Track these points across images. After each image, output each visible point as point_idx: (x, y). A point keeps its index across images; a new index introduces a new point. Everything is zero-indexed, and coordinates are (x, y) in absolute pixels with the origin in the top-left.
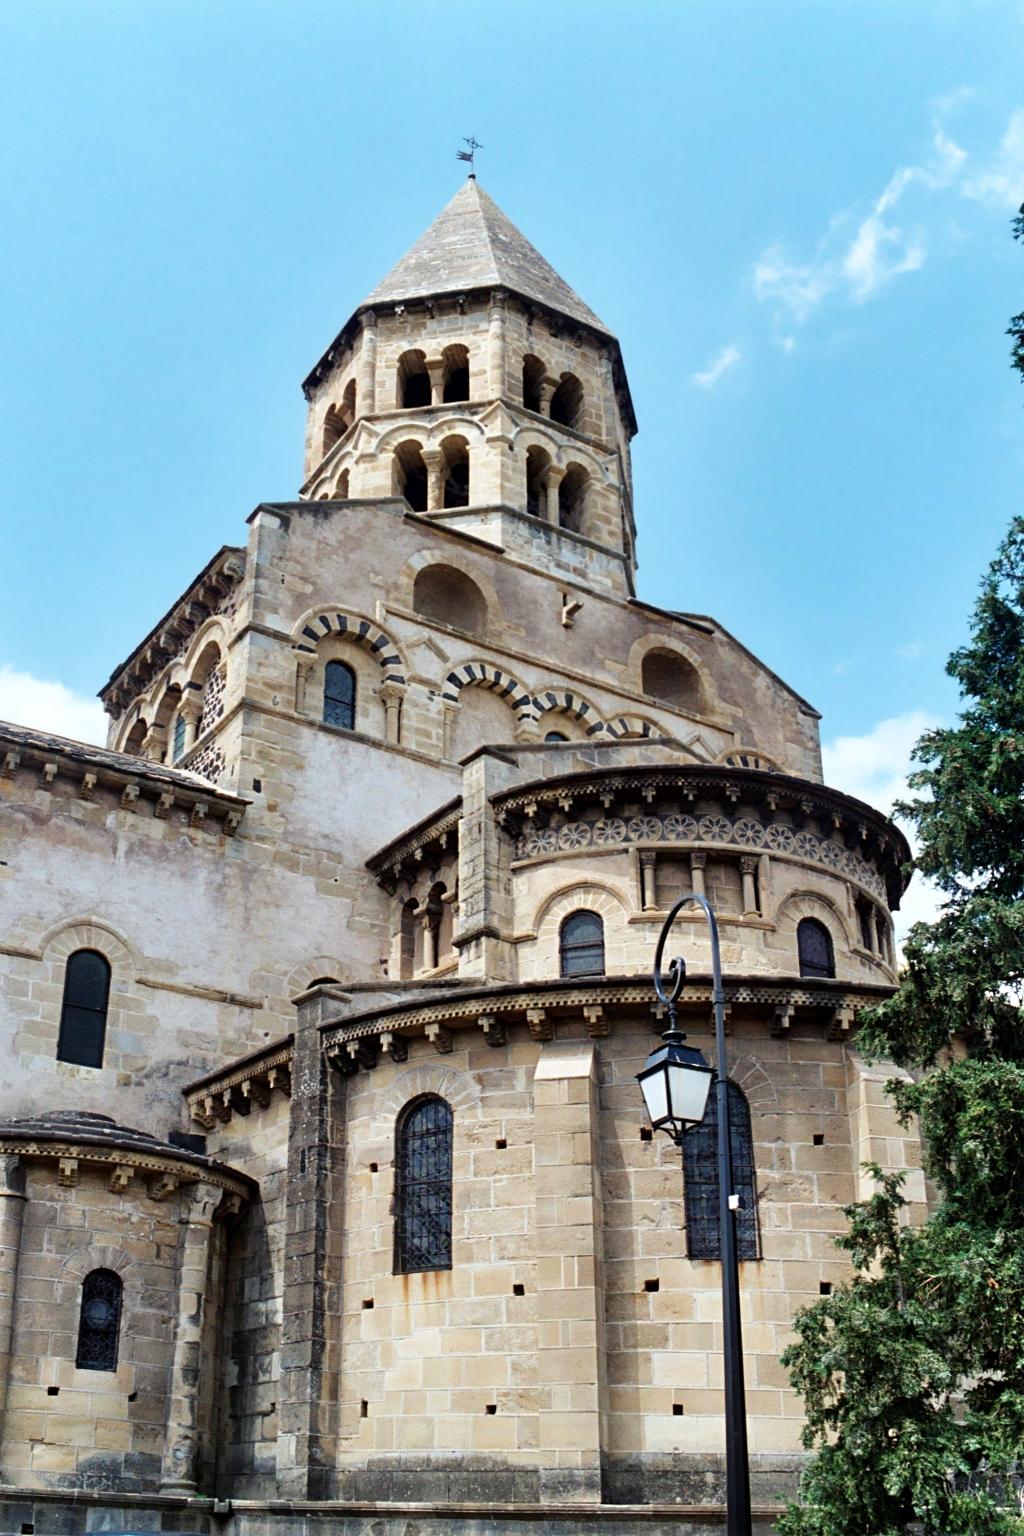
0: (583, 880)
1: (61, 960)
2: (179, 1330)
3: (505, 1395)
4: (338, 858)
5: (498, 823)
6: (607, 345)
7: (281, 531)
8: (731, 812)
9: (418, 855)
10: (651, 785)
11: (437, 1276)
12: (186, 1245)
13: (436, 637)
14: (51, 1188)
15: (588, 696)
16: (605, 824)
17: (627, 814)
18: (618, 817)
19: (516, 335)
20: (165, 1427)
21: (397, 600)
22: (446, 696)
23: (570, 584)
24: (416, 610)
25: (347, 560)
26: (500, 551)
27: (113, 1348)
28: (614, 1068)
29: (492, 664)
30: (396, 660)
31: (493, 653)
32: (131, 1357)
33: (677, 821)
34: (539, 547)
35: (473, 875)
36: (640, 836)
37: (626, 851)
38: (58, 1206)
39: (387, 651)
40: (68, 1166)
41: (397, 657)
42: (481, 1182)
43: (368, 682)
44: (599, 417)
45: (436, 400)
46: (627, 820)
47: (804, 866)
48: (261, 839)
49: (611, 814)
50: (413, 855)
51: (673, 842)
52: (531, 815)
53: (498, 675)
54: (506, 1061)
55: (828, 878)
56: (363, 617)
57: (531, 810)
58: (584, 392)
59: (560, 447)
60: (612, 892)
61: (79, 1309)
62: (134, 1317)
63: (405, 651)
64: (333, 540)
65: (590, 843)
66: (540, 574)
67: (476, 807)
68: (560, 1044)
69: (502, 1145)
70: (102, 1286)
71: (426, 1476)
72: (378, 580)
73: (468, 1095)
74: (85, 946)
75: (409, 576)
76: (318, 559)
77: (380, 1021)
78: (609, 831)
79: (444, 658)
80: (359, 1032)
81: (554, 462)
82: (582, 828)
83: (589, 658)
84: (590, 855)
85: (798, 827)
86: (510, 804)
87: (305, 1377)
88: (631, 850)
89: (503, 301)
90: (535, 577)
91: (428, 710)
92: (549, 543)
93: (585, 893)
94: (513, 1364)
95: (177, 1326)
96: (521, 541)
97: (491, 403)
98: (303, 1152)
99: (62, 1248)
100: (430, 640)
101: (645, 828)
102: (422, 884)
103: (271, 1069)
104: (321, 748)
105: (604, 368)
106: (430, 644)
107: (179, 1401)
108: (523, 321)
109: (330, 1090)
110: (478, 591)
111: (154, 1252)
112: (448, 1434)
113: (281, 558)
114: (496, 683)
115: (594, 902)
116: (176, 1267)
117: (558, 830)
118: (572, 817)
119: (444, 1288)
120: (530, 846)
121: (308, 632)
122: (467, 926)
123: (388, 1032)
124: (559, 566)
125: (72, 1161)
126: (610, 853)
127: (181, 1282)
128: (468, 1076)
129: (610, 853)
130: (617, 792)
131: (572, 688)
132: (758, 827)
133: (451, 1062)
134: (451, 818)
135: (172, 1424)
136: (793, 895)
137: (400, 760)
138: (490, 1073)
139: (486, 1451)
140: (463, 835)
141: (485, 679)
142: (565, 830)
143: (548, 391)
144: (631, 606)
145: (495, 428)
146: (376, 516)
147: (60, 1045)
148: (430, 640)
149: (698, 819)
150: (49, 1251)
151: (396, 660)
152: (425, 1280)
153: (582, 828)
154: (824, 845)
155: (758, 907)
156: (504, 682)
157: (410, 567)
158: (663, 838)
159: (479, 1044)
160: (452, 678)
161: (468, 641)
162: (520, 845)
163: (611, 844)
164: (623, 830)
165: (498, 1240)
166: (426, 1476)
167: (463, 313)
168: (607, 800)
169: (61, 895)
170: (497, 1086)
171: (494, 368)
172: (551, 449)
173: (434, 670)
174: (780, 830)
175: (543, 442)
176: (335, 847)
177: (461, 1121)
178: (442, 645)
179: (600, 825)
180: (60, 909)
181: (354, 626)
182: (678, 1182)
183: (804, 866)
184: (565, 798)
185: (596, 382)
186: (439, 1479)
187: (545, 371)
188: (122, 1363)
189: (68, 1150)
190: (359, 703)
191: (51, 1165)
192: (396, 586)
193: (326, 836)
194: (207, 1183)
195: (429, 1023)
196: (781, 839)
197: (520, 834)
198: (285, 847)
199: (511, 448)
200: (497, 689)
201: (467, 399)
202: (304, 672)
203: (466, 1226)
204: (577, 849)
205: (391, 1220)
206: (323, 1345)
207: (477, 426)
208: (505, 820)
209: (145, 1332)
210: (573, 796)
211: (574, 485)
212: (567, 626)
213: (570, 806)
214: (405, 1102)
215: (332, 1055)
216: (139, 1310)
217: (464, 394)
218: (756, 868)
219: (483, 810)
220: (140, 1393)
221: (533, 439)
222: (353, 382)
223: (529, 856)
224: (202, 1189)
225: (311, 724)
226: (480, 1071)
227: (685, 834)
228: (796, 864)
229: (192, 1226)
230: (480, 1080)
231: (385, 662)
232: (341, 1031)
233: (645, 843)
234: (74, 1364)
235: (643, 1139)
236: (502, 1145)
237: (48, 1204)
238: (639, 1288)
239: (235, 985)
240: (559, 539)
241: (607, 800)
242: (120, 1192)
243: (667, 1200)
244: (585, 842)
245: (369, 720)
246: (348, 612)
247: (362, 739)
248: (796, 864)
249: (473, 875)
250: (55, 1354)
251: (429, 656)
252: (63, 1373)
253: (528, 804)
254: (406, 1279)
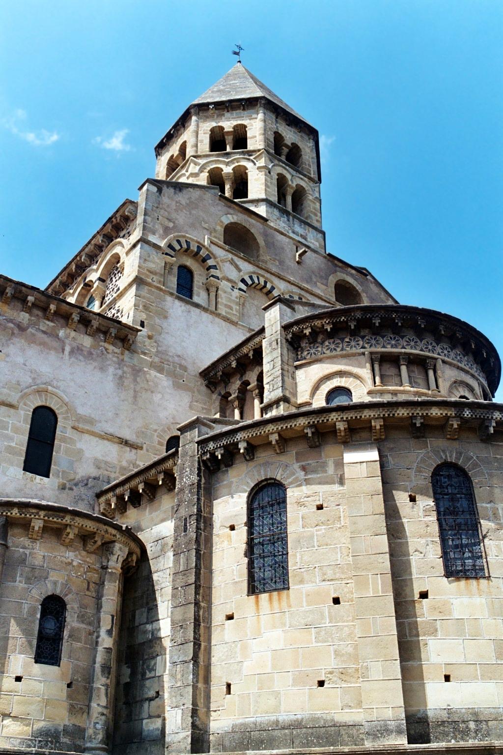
0: (339, 370)
1: (29, 411)
2: (100, 640)
3: (331, 673)
4: (185, 369)
5: (287, 340)
6: (312, 133)
7: (158, 194)
8: (420, 334)
9: (234, 365)
10: (377, 316)
11: (279, 595)
12: (105, 583)
13: (235, 258)
14: (24, 540)
16: (350, 339)
17: (362, 334)
18: (358, 336)
19: (270, 122)
20: (89, 706)
21: (215, 237)
22: (240, 289)
23: (299, 242)
24: (225, 243)
25: (190, 214)
26: (265, 220)
27: (58, 650)
28: (390, 458)
29: (263, 276)
30: (215, 267)
31: (263, 271)
32: (70, 657)
33: (391, 338)
34: (284, 222)
35: (273, 368)
36: (371, 346)
37: (364, 354)
38: (27, 552)
39: (210, 262)
40: (37, 524)
41: (215, 266)
42: (308, 531)
43: (199, 279)
44: (310, 166)
45: (228, 149)
46: (363, 337)
47: (458, 368)
48: (145, 354)
49: (354, 334)
50: (230, 364)
51: (389, 349)
52: (308, 334)
53: (266, 283)
54: (321, 455)
56: (198, 242)
57: (307, 332)
58: (303, 153)
59: (293, 176)
60: (357, 377)
61: (38, 622)
62: (73, 630)
63: (220, 263)
64: (183, 202)
65: (342, 350)
67: (274, 331)
68: (355, 445)
69: (320, 507)
70: (53, 607)
71: (277, 733)
72: (206, 226)
73: (297, 478)
74: (44, 404)
75: (221, 226)
76: (176, 210)
77: (239, 434)
78: (353, 343)
79: (239, 270)
80: (224, 442)
81: (290, 183)
82: (336, 342)
83: (309, 280)
84: (343, 356)
85: (453, 347)
86: (295, 328)
87: (188, 668)
88: (366, 353)
89: (264, 104)
90: (282, 236)
91: (231, 296)
92: (288, 220)
93: (340, 377)
94: (336, 651)
95: (98, 637)
96: (275, 217)
97: (259, 150)
98: (186, 519)
99: (28, 580)
100: (232, 259)
101: (373, 342)
102: (234, 383)
103: (160, 473)
104: (176, 308)
105: (311, 144)
106: (232, 262)
107: (99, 689)
108: (274, 117)
109: (203, 481)
110: (255, 239)
111: (85, 586)
112: (296, 704)
113: (157, 207)
114: (265, 286)
115: (346, 382)
116: (99, 597)
117: (322, 343)
118: (331, 335)
119: (284, 603)
120: (306, 353)
121: (170, 246)
122: (270, 397)
123: (244, 440)
124: (294, 232)
125: (41, 521)
126: (354, 355)
127: (101, 607)
128: (296, 466)
129: (354, 355)
130: (358, 321)
132: (434, 344)
133: (283, 459)
134: (257, 340)
135: (94, 705)
136: (455, 382)
137: (217, 320)
138: (311, 464)
139: (318, 713)
140: (266, 348)
141: (259, 283)
142: (327, 343)
143: (285, 150)
144: (328, 257)
145: (262, 162)
146: (205, 194)
147: (25, 462)
148: (232, 259)
149: (402, 337)
150: (20, 582)
151: (215, 267)
152: (270, 599)
153: (336, 342)
155: (437, 387)
156: (269, 286)
157: (222, 222)
158: (384, 347)
159: (302, 447)
160: (243, 281)
161: (250, 262)
162: (299, 353)
163: (354, 350)
164: (361, 343)
165: (321, 567)
166: (277, 733)
167: (244, 109)
168: (353, 325)
169: (31, 372)
170: (314, 471)
171: (260, 134)
172: (289, 177)
173: (234, 275)
174: (445, 347)
175: (285, 172)
176: (183, 362)
178: (238, 263)
179: (347, 340)
180: (30, 381)
181: (194, 248)
182: (435, 528)
184: (328, 324)
185: (308, 150)
186: (285, 735)
187: (284, 140)
188: (64, 660)
189: (37, 513)
190: (195, 289)
191: (26, 526)
192: (215, 230)
193: (179, 356)
194: (120, 543)
195: (272, 433)
196: (446, 352)
197: (299, 346)
198: (157, 360)
199: (269, 173)
200: (265, 290)
201: (247, 148)
202: (168, 267)
204: (334, 353)
205: (246, 560)
206: (200, 645)
207: (253, 162)
208: (291, 338)
209: (78, 640)
210: (333, 323)
211: (299, 196)
212: (298, 263)
213: (331, 328)
214: (253, 485)
215: (205, 458)
216: (76, 624)
217: (245, 146)
218: (435, 366)
219: (279, 332)
220: (74, 682)
221: (279, 170)
222: (185, 142)
223: (305, 359)
224: (117, 546)
225: (172, 294)
226: (303, 463)
227: (395, 345)
229: (110, 571)
230: (304, 468)
231: (208, 269)
232: (212, 443)
233: (373, 349)
234: (33, 660)
235: (411, 501)
236: (320, 507)
237: (21, 550)
238: (417, 596)
239: (127, 435)
240: (293, 220)
241: (353, 325)
242: (69, 546)
243: (430, 539)
244: (339, 349)
245: (200, 296)
246: (190, 238)
247: (197, 306)
249: (273, 368)
250: (20, 653)
251: (231, 268)
252: (25, 666)
253: (306, 328)
254: (257, 598)
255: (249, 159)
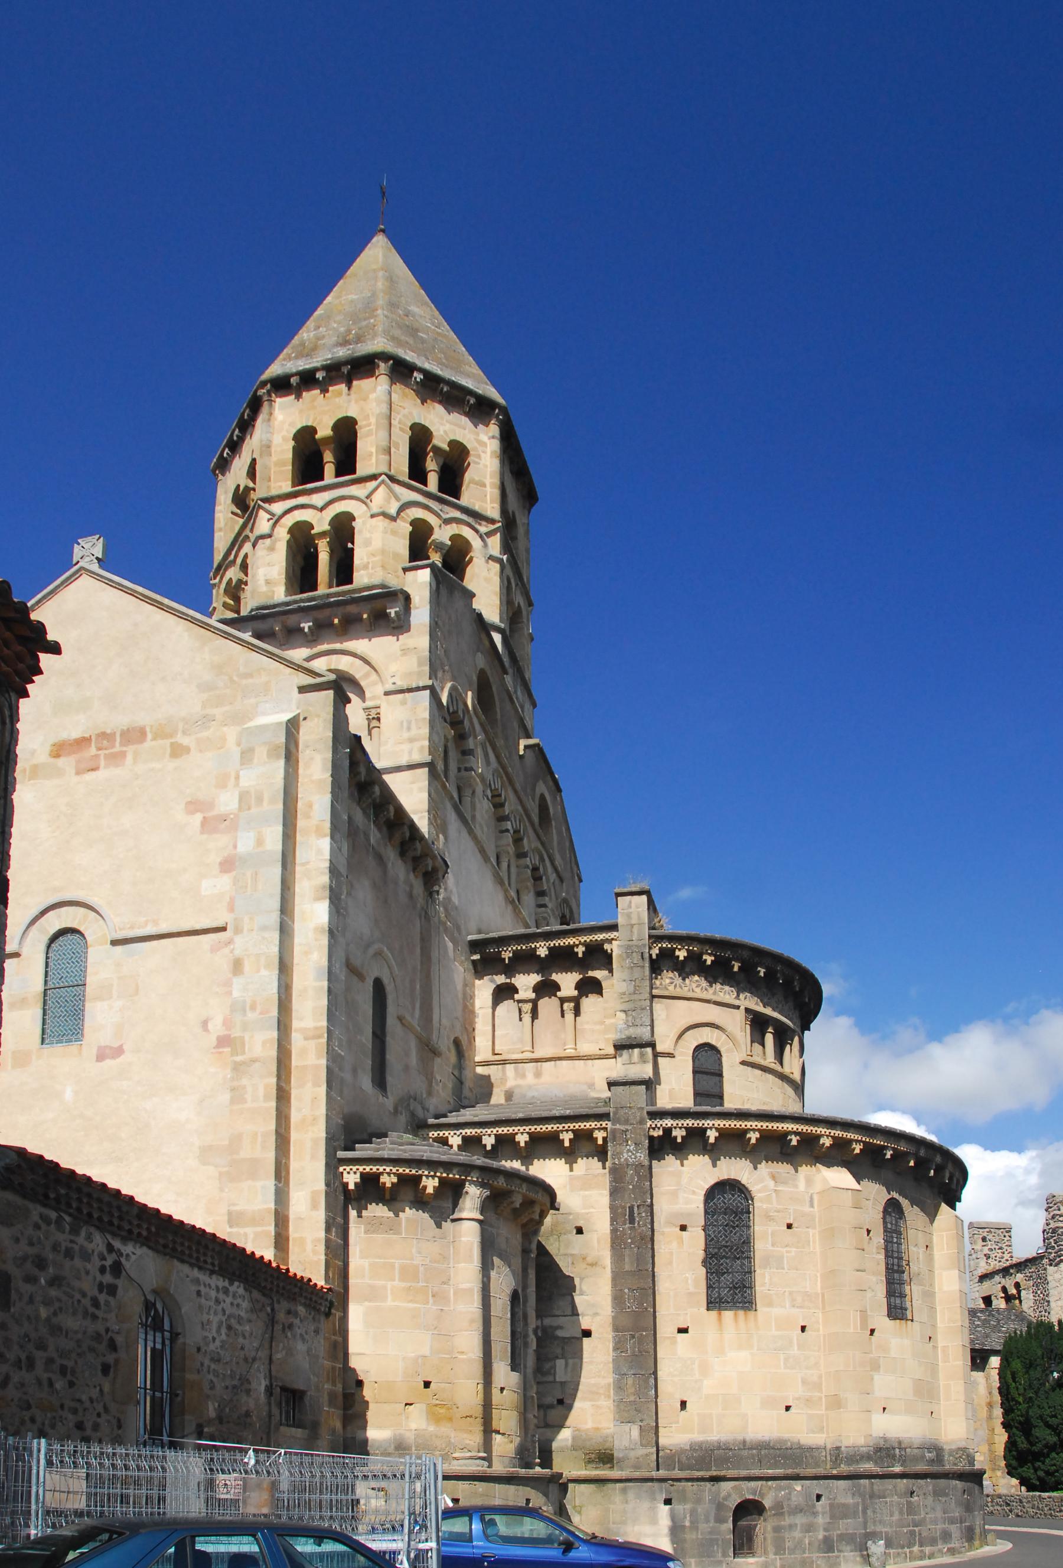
3: (798, 1399)
52: (681, 958)
69: (789, 1226)
71: (745, 1453)
134: (600, 937)
139: (786, 1436)
165: (791, 1293)
166: (745, 1453)
170: (784, 1183)
177: (759, 1206)
186: (753, 1455)
203: (767, 1280)
230: (773, 1177)
254: (720, 1314)
255: (477, 531)
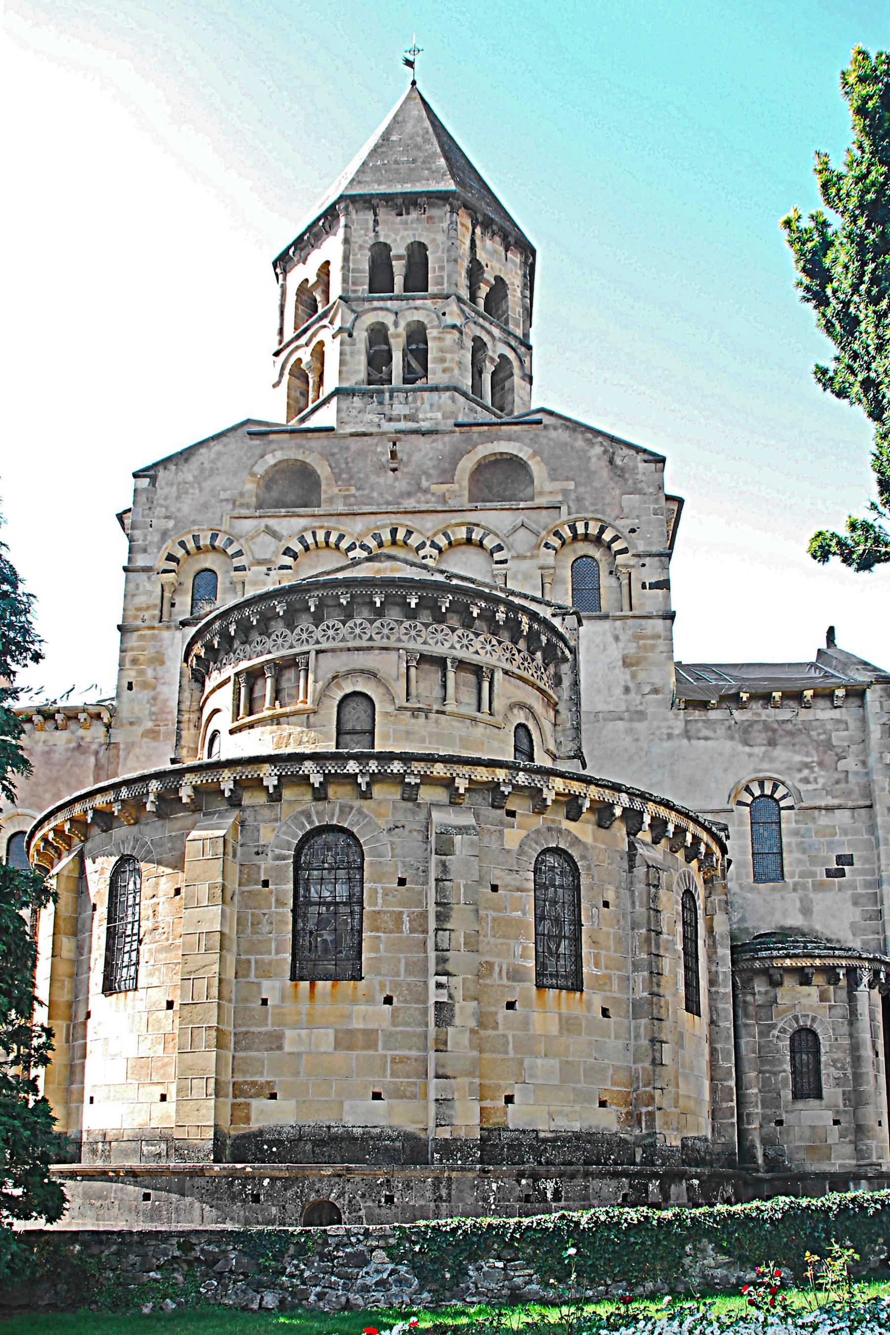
13: (271, 522)
15: (409, 523)
26: (332, 429)
47: (349, 649)
55: (377, 652)
66: (371, 434)
79: (274, 534)
90: (366, 438)
92: (381, 403)
131: (395, 521)
136: (334, 678)
144: (457, 429)
154: (377, 624)
183: (349, 649)
228: (341, 650)
248: (341, 650)
